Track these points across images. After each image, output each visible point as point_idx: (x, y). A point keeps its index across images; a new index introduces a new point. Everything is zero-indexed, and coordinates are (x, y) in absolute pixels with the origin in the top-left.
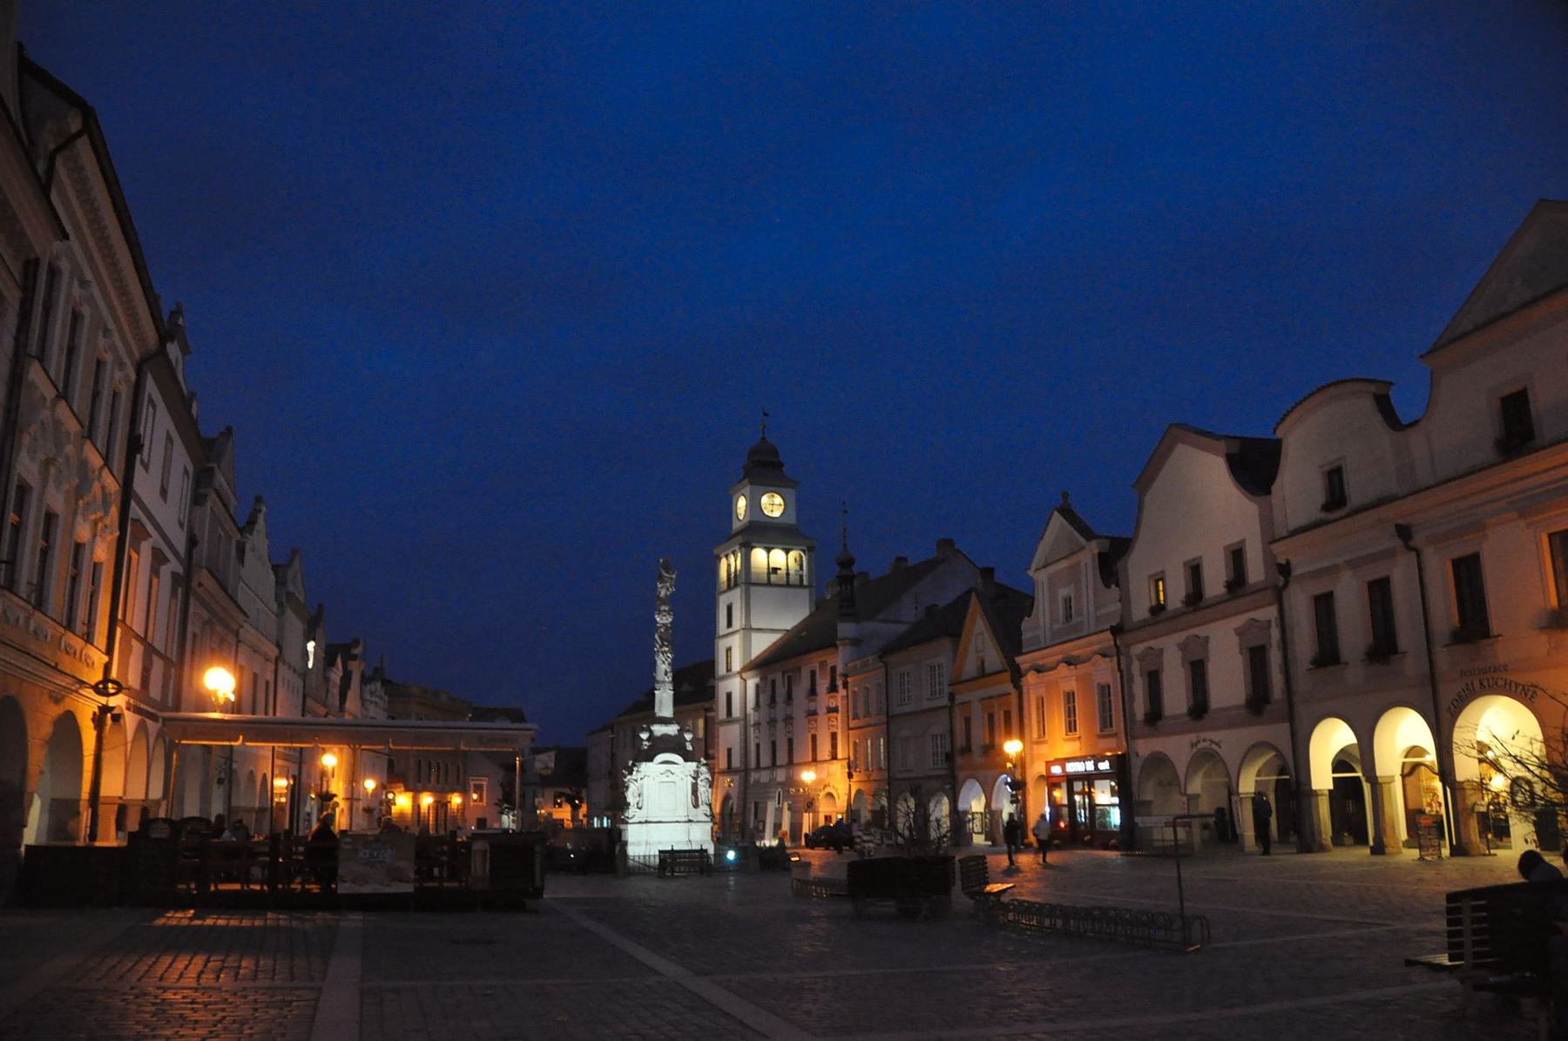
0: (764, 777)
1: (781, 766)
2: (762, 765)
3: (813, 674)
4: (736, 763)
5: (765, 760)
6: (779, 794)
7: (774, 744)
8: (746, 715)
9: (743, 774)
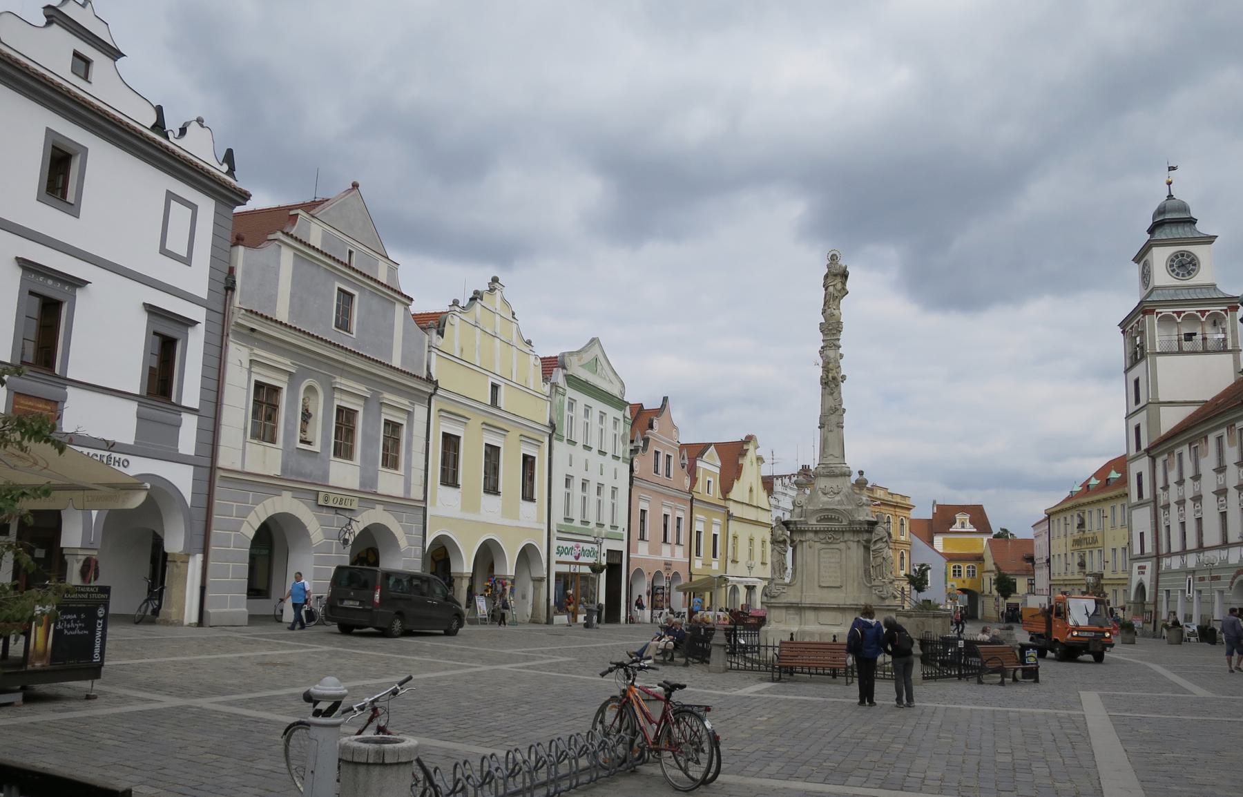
0: (1175, 563)
1: (1191, 551)
2: (1173, 550)
3: (1220, 439)
4: (1149, 549)
5: (1176, 547)
6: (1190, 581)
7: (1183, 524)
8: (1155, 497)
9: (1155, 559)
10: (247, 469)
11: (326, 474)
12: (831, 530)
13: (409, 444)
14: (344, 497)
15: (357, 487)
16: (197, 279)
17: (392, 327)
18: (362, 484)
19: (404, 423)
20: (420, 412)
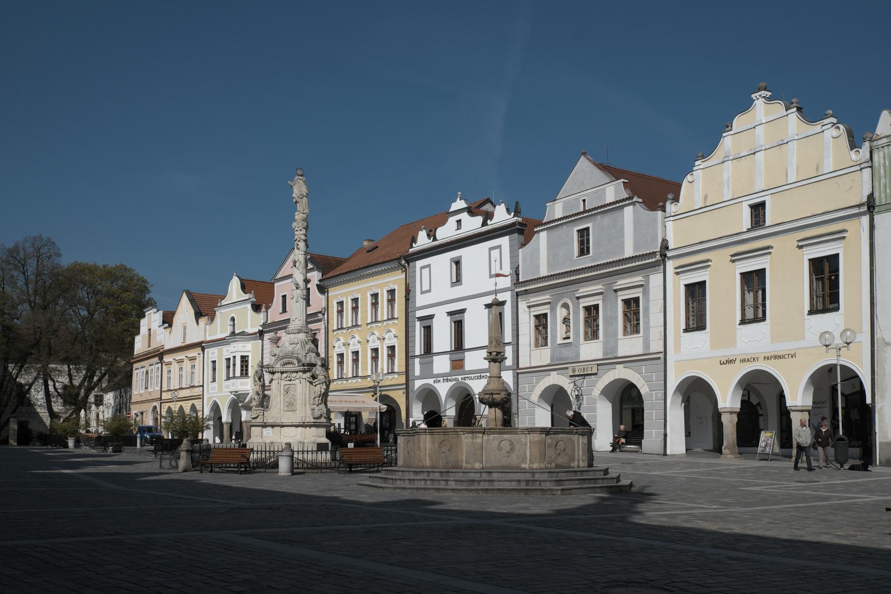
10: (532, 366)
11: (578, 354)
12: (288, 372)
13: (647, 309)
14: (586, 367)
15: (600, 356)
16: (506, 282)
17: (622, 228)
18: (604, 354)
19: (640, 295)
20: (655, 279)
